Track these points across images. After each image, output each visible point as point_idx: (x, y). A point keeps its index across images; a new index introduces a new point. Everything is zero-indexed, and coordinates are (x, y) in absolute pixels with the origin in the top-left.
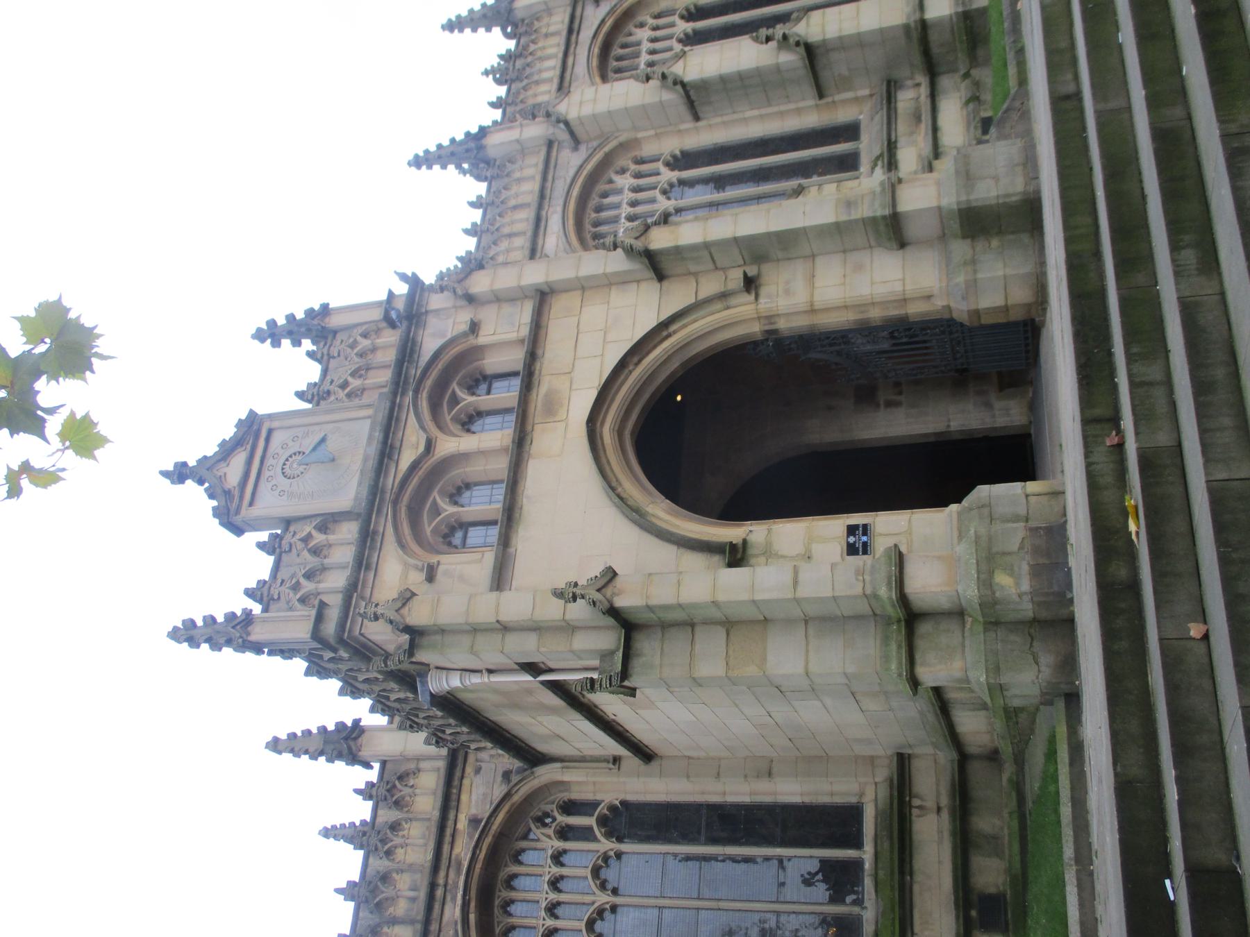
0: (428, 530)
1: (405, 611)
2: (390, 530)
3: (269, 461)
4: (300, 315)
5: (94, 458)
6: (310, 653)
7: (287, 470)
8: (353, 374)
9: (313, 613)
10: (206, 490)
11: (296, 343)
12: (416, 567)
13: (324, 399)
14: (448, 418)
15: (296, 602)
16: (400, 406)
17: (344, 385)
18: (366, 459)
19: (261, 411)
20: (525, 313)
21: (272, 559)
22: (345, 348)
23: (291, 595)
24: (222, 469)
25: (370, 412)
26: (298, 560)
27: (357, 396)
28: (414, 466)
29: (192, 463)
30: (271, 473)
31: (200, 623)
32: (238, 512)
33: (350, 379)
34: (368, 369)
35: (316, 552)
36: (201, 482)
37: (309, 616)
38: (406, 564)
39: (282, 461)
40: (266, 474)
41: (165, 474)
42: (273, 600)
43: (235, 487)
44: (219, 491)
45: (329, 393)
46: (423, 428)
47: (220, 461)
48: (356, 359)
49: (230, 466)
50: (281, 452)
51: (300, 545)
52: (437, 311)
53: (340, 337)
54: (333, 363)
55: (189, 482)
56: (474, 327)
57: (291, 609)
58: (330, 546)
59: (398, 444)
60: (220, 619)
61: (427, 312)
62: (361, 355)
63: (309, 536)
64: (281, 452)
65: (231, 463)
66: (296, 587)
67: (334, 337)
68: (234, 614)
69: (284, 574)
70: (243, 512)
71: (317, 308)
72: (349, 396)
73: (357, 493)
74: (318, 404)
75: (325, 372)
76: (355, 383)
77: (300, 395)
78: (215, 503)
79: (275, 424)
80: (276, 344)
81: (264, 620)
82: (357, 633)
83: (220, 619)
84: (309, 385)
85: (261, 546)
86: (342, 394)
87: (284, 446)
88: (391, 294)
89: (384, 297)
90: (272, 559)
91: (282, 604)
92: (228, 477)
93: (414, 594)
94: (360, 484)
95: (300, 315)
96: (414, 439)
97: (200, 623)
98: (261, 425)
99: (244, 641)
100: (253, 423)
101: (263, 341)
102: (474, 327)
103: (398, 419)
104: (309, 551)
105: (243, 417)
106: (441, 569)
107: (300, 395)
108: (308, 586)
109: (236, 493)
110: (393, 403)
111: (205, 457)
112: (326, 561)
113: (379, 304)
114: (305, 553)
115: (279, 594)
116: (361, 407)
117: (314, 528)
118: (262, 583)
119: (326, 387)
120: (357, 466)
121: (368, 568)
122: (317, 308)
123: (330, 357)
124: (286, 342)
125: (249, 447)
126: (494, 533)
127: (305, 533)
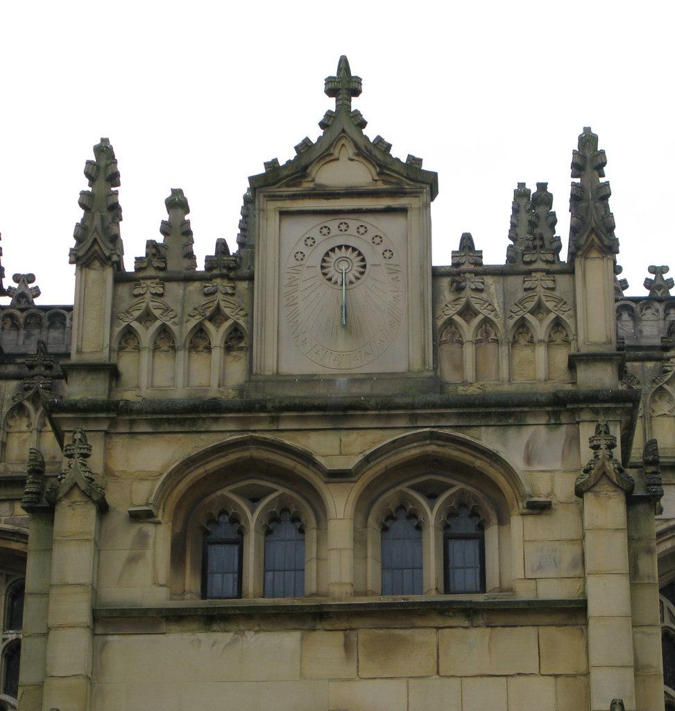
0: (225, 492)
1: (76, 496)
3: (354, 223)
7: (333, 256)
14: (403, 487)
15: (125, 324)
20: (554, 590)
22: (536, 298)
23: (137, 314)
28: (307, 458)
30: (335, 230)
32: (273, 197)
35: (200, 331)
39: (352, 242)
40: (333, 224)
43: (313, 180)
46: (368, 460)
47: (356, 146)
49: (350, 161)
50: (369, 237)
56: (540, 508)
65: (354, 163)
66: (147, 317)
75: (496, 272)
87: (377, 239)
102: (540, 508)
103: (389, 417)
106: (149, 528)
108: (146, 335)
109: (306, 185)
115: (140, 295)
125: (381, 186)
126: (191, 600)
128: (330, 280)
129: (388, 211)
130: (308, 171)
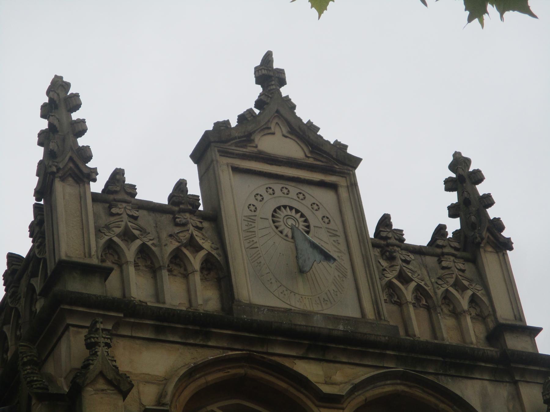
1: (101, 385)
2: (210, 355)
3: (294, 189)
4: (492, 213)
5: (311, 8)
6: (39, 260)
7: (284, 213)
8: (419, 288)
9: (95, 261)
10: (250, 111)
11: (453, 211)
12: (161, 396)
13: (383, 254)
15: (107, 238)
16: (382, 357)
17: (404, 278)
18: (306, 315)
19: (360, 172)
21: (166, 202)
22: (454, 276)
23: (118, 231)
24: (280, 130)
25: (370, 315)
26: (164, 235)
27: (390, 296)
29: (284, 91)
30: (278, 192)
31: (75, 116)
32: (225, 153)
33: (413, 285)
34: (428, 308)
36: (259, 104)
37: (90, 256)
38: (166, 380)
40: (277, 186)
41: (268, 58)
42: (110, 208)
43: (256, 147)
44: (250, 128)
45: (391, 258)
46: (356, 388)
48: (440, 292)
49: (283, 138)
50: (308, 202)
51: (184, 237)
52: (517, 396)
53: (469, 268)
54: (431, 261)
55: (259, 89)
57: (98, 231)
58: (186, 276)
59: (330, 357)
60: (82, 142)
61: (515, 383)
62: (447, 297)
63: (197, 248)
64: (308, 202)
65: (288, 140)
67: (467, 260)
68: (89, 158)
69: (144, 216)
70: (224, 160)
71: (505, 234)
72: (390, 285)
73: (259, 307)
74: (375, 245)
76: (408, 292)
77: (385, 221)
78: (234, 123)
79: (343, 193)
80: (450, 185)
81: (82, 197)
82: (69, 321)
83: (82, 142)
84: (400, 232)
85: (181, 186)
86: (391, 275)
87: (315, 206)
88: (536, 331)
89: (530, 321)
90: (166, 202)
91: (104, 220)
92: (270, 137)
93: (124, 395)
94: (272, 309)
95: (492, 213)
96: (338, 377)
97: (75, 116)
98: (341, 174)
99: (53, 173)
100: (344, 164)
101: (452, 167)
104: (178, 249)
105: (349, 151)
107: (385, 221)
109: (249, 150)
110: (386, 346)
111: (294, 107)
112: (165, 273)
113: (519, 315)
114: (174, 245)
115: (118, 214)
116: (376, 304)
117: (209, 254)
118: (132, 190)
119: (400, 255)
120: (296, 304)
121: (158, 329)
122: (505, 234)
123: (440, 257)
124: (453, 197)
125: (311, 161)
127: (200, 242)
128: (281, 232)
129: (322, 184)
130: (252, 138)
